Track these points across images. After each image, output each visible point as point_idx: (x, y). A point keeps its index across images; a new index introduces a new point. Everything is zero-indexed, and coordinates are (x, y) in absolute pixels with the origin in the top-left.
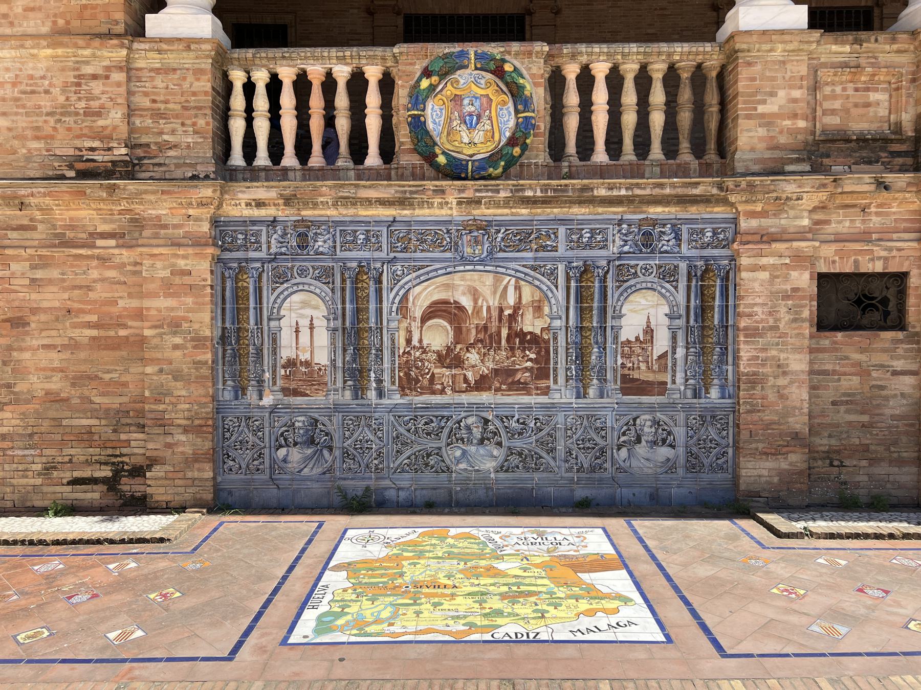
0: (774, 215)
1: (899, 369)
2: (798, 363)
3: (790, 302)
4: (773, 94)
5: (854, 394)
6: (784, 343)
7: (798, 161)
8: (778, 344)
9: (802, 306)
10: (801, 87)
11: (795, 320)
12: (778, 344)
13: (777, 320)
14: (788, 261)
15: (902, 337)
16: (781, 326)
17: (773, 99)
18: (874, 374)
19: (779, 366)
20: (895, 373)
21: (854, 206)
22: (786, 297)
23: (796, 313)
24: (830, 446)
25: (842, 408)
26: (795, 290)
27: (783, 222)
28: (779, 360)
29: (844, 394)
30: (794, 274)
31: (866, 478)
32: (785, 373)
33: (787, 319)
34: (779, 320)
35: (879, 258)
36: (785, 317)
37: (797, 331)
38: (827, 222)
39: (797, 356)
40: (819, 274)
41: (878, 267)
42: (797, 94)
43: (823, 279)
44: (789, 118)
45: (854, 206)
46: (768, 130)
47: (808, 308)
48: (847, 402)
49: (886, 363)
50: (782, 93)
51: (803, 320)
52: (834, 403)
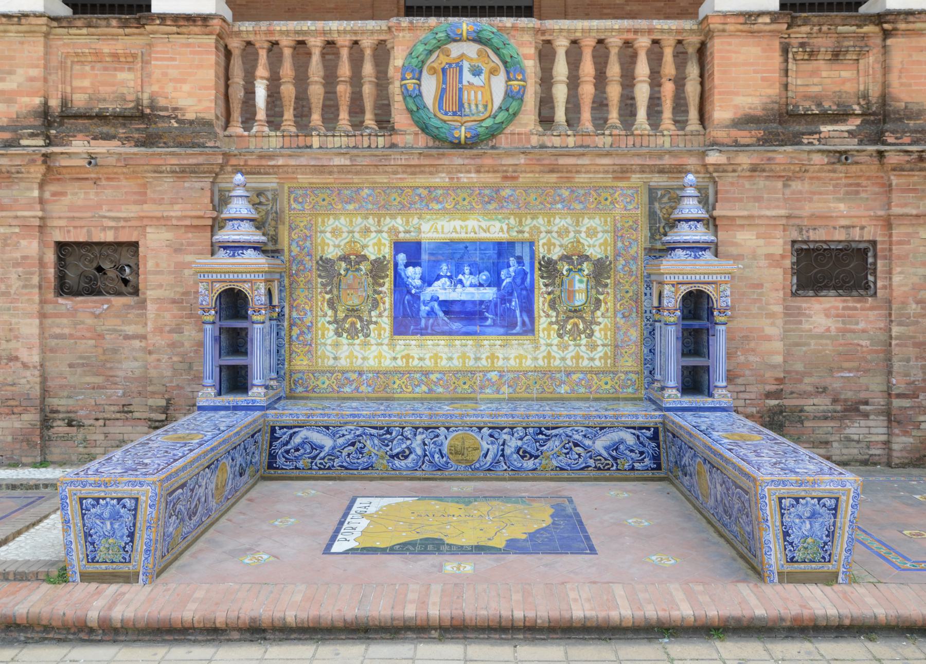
0: (7, 186)
1: (130, 333)
2: (30, 328)
3: (20, 269)
4: (11, 72)
5: (89, 357)
6: (15, 309)
7: (32, 135)
8: (9, 309)
9: (33, 274)
10: (37, 67)
11: (25, 287)
12: (9, 309)
13: (9, 286)
14: (17, 230)
15: (132, 303)
16: (12, 292)
17: (13, 77)
18: (107, 337)
19: (11, 330)
20: (127, 337)
21: (87, 179)
22: (16, 264)
23: (26, 280)
24: (68, 405)
25: (79, 370)
26: (25, 258)
27: (15, 193)
28: (11, 324)
29: (81, 357)
30: (24, 243)
31: (102, 437)
32: (16, 338)
33: (17, 285)
34: (10, 286)
35: (111, 228)
36: (16, 284)
37: (26, 297)
38: (63, 194)
39: (28, 321)
40: (56, 242)
41: (109, 237)
42: (34, 72)
43: (62, 247)
44: (27, 96)
45: (87, 179)
46: (8, 106)
47: (37, 274)
48: (83, 365)
49: (119, 328)
50: (20, 71)
51: (33, 287)
52: (71, 366)
